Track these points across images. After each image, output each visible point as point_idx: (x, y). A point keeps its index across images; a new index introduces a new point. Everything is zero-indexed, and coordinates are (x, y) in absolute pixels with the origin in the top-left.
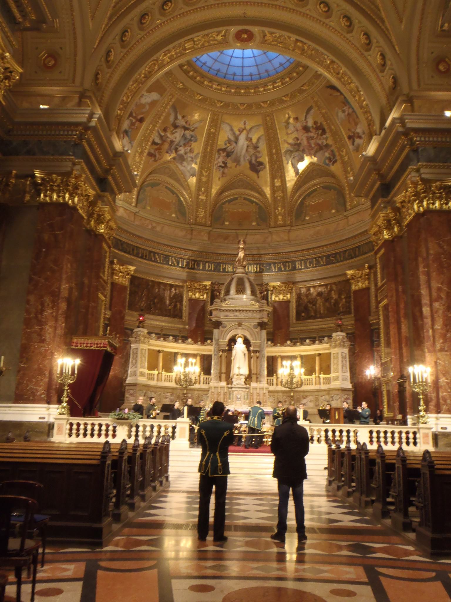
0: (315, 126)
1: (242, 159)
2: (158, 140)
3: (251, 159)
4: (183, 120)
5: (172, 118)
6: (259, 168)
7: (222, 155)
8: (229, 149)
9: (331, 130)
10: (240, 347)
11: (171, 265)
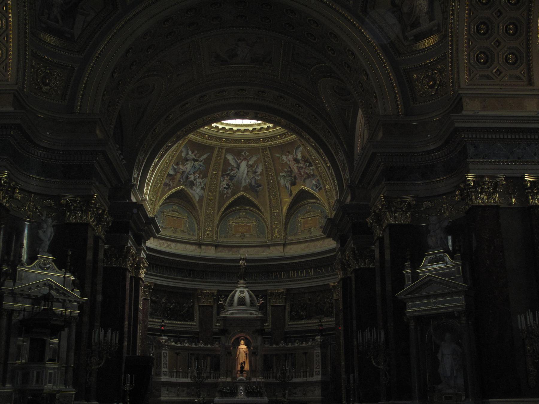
0: (303, 160)
1: (243, 182)
2: (172, 172)
3: (251, 182)
4: (193, 154)
5: (184, 155)
6: (258, 189)
7: (226, 179)
8: (232, 173)
9: (316, 165)
10: (243, 347)
11: (184, 277)
